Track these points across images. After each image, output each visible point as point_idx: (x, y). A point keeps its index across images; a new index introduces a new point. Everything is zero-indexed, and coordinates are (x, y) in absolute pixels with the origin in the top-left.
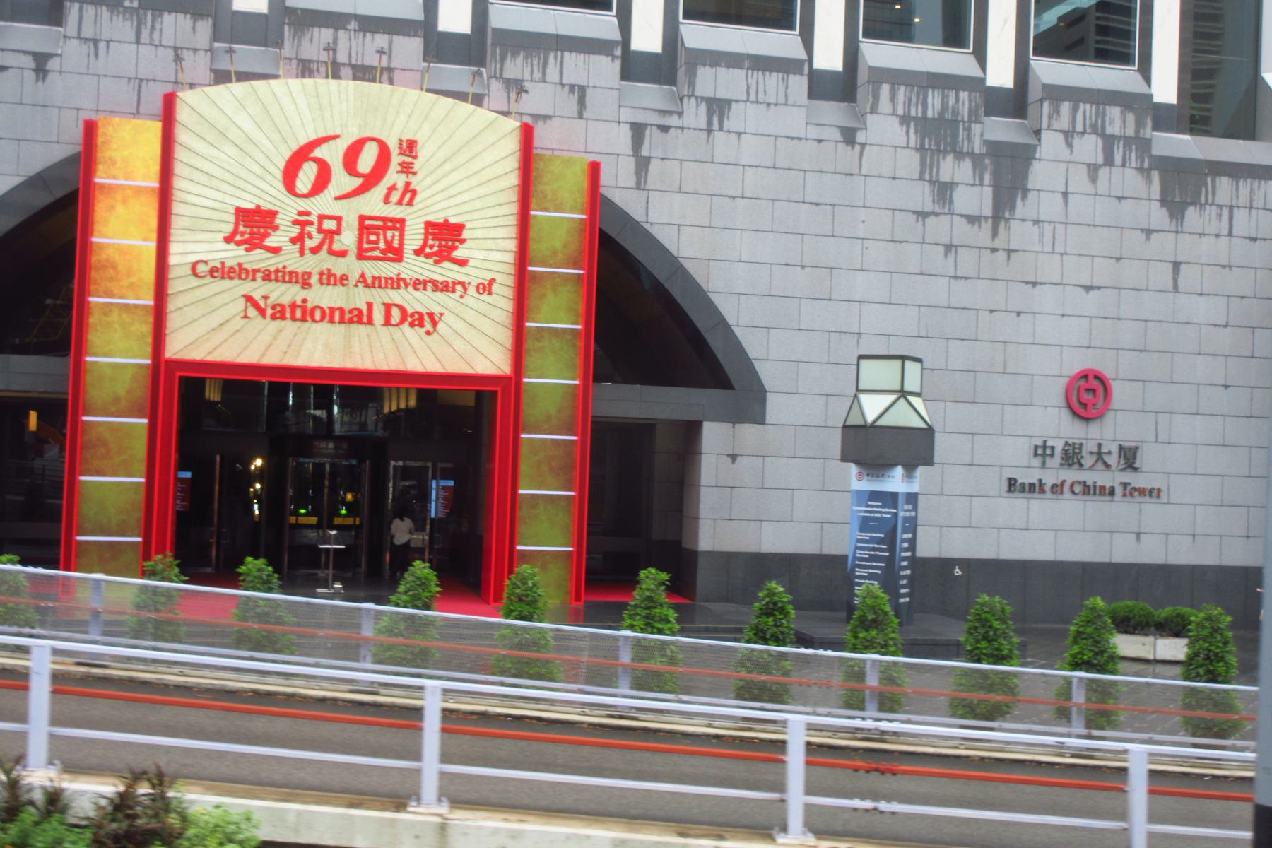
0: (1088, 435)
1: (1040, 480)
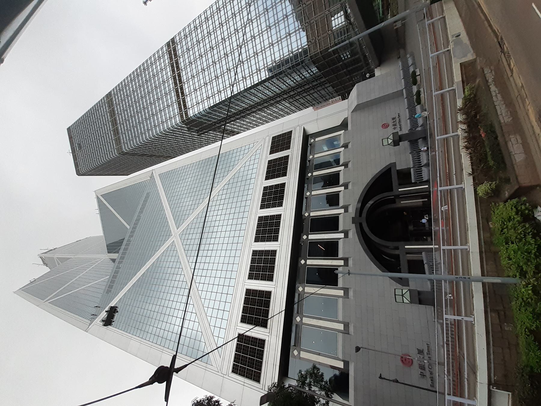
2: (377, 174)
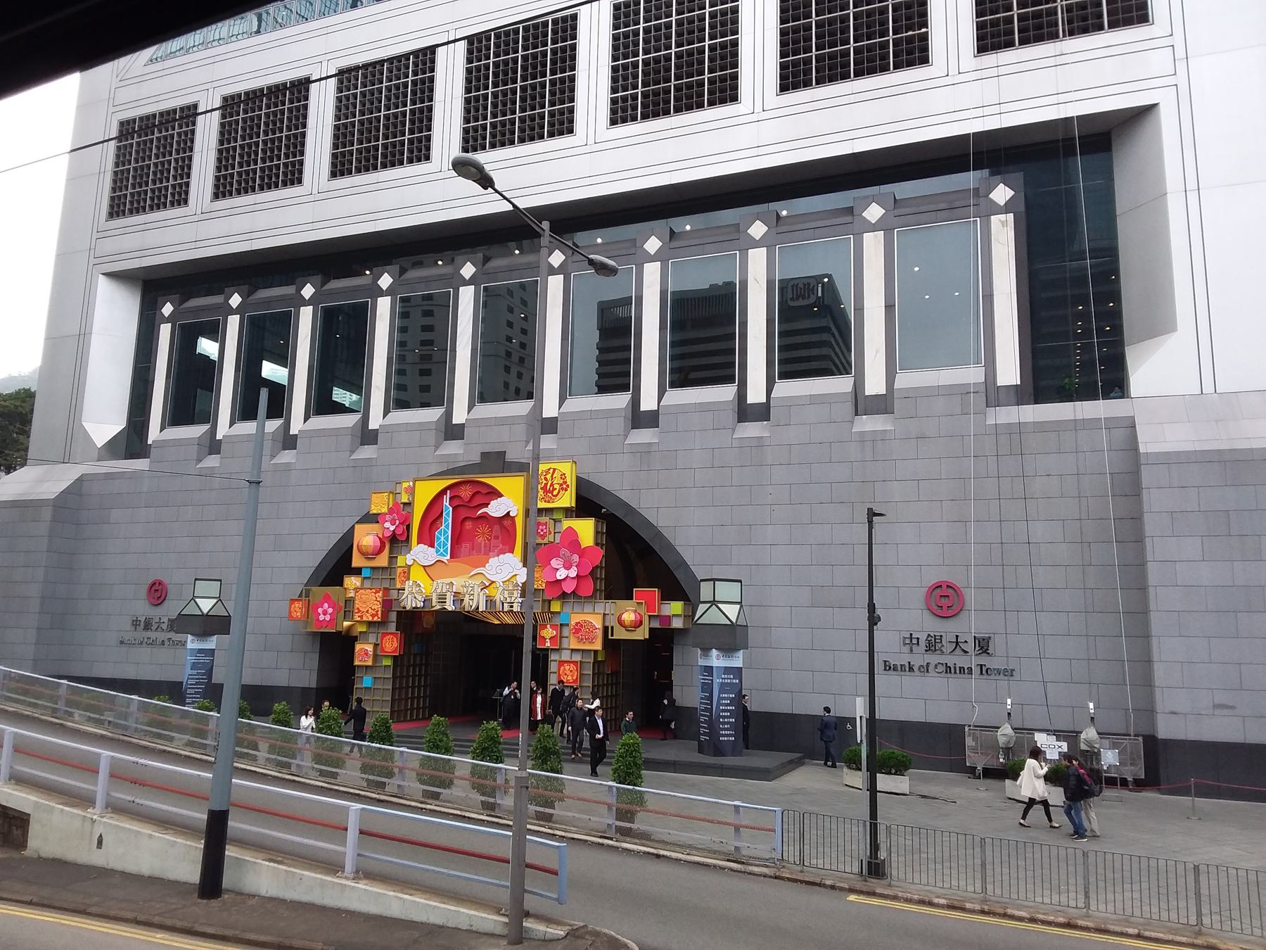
0: (947, 629)
1: (909, 663)
2: (671, 548)
